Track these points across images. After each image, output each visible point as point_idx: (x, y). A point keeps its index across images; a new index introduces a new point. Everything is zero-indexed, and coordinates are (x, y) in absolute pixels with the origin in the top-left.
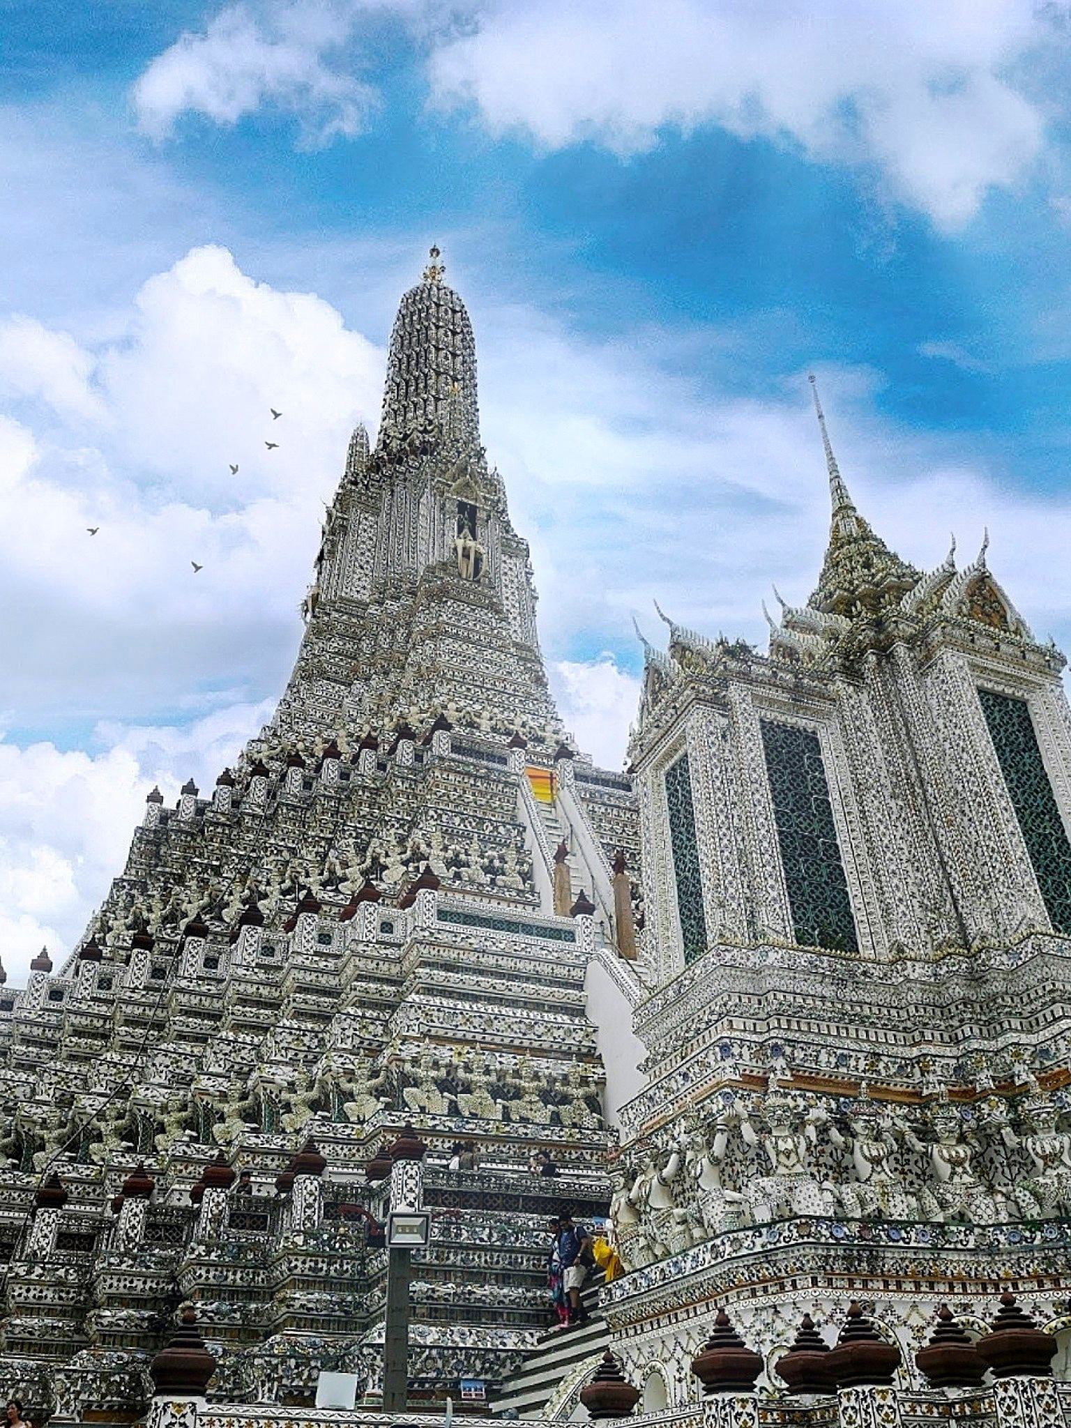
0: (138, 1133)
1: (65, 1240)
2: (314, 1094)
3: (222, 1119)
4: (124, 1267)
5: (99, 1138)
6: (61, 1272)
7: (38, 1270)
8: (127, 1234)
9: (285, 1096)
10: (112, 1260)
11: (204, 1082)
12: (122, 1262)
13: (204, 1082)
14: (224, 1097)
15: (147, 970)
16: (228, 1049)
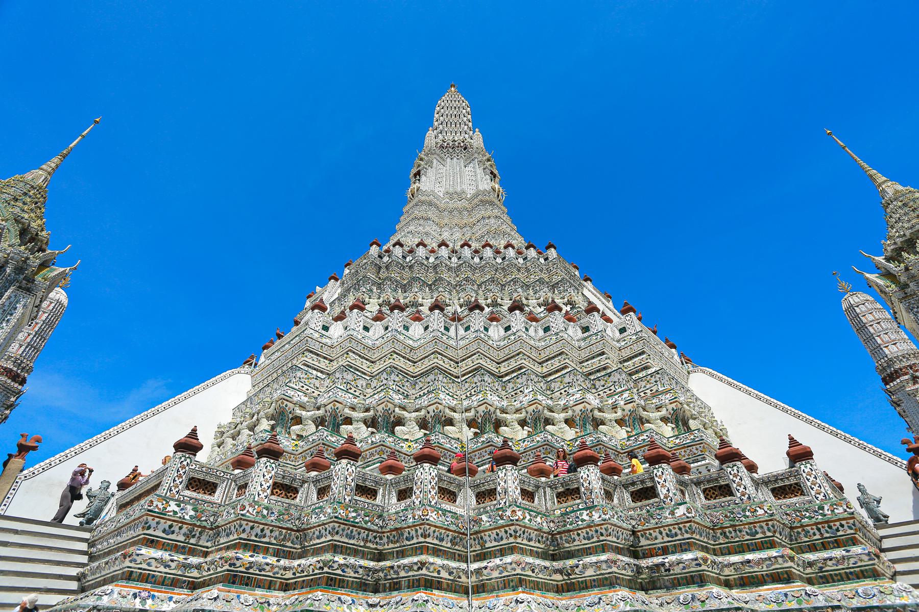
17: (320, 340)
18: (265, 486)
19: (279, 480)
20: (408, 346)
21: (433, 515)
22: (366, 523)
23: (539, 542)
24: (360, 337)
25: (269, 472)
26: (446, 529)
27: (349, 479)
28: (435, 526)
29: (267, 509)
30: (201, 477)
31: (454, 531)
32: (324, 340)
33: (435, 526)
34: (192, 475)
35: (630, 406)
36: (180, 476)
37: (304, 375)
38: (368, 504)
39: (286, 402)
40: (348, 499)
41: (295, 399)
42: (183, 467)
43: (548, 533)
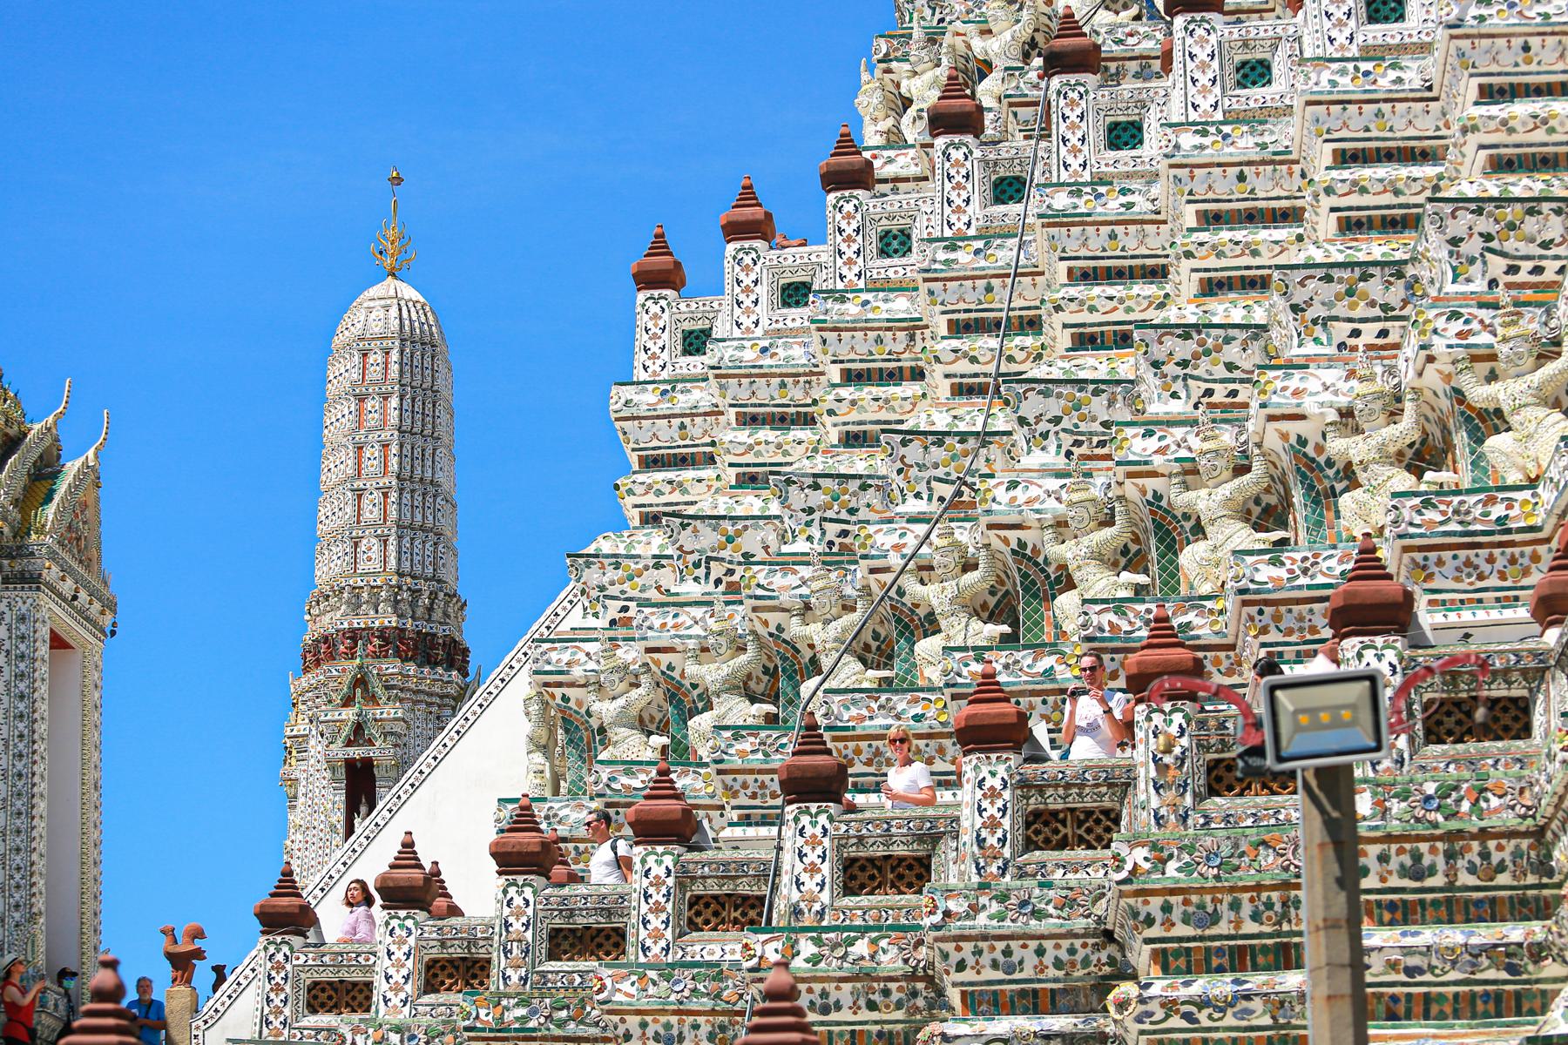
0: (1018, 594)
1: (859, 874)
2: (1405, 429)
3: (1199, 531)
4: (982, 919)
5: (930, 625)
6: (861, 948)
7: (807, 948)
8: (981, 842)
9: (1338, 446)
10: (952, 905)
11: (1138, 446)
12: (975, 909)
13: (1138, 446)
14: (1190, 472)
15: (977, 190)
16: (1184, 349)
17: (664, 408)
18: (398, 978)
19: (435, 953)
20: (892, 325)
21: (625, 986)
22: (561, 1024)
23: (872, 1006)
24: (749, 355)
25: (402, 942)
26: (675, 1013)
27: (517, 926)
28: (638, 1012)
29: (398, 1030)
30: (326, 976)
31: (713, 1012)
32: (683, 402)
33: (638, 1012)
34: (307, 978)
35: (1432, 378)
36: (278, 989)
37: (612, 574)
38: (582, 973)
39: (558, 692)
40: (515, 977)
41: (577, 673)
42: (279, 967)
43: (912, 977)
